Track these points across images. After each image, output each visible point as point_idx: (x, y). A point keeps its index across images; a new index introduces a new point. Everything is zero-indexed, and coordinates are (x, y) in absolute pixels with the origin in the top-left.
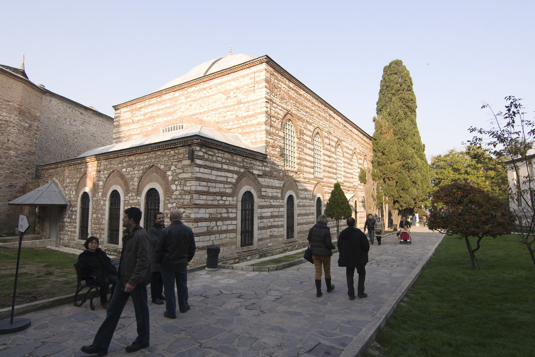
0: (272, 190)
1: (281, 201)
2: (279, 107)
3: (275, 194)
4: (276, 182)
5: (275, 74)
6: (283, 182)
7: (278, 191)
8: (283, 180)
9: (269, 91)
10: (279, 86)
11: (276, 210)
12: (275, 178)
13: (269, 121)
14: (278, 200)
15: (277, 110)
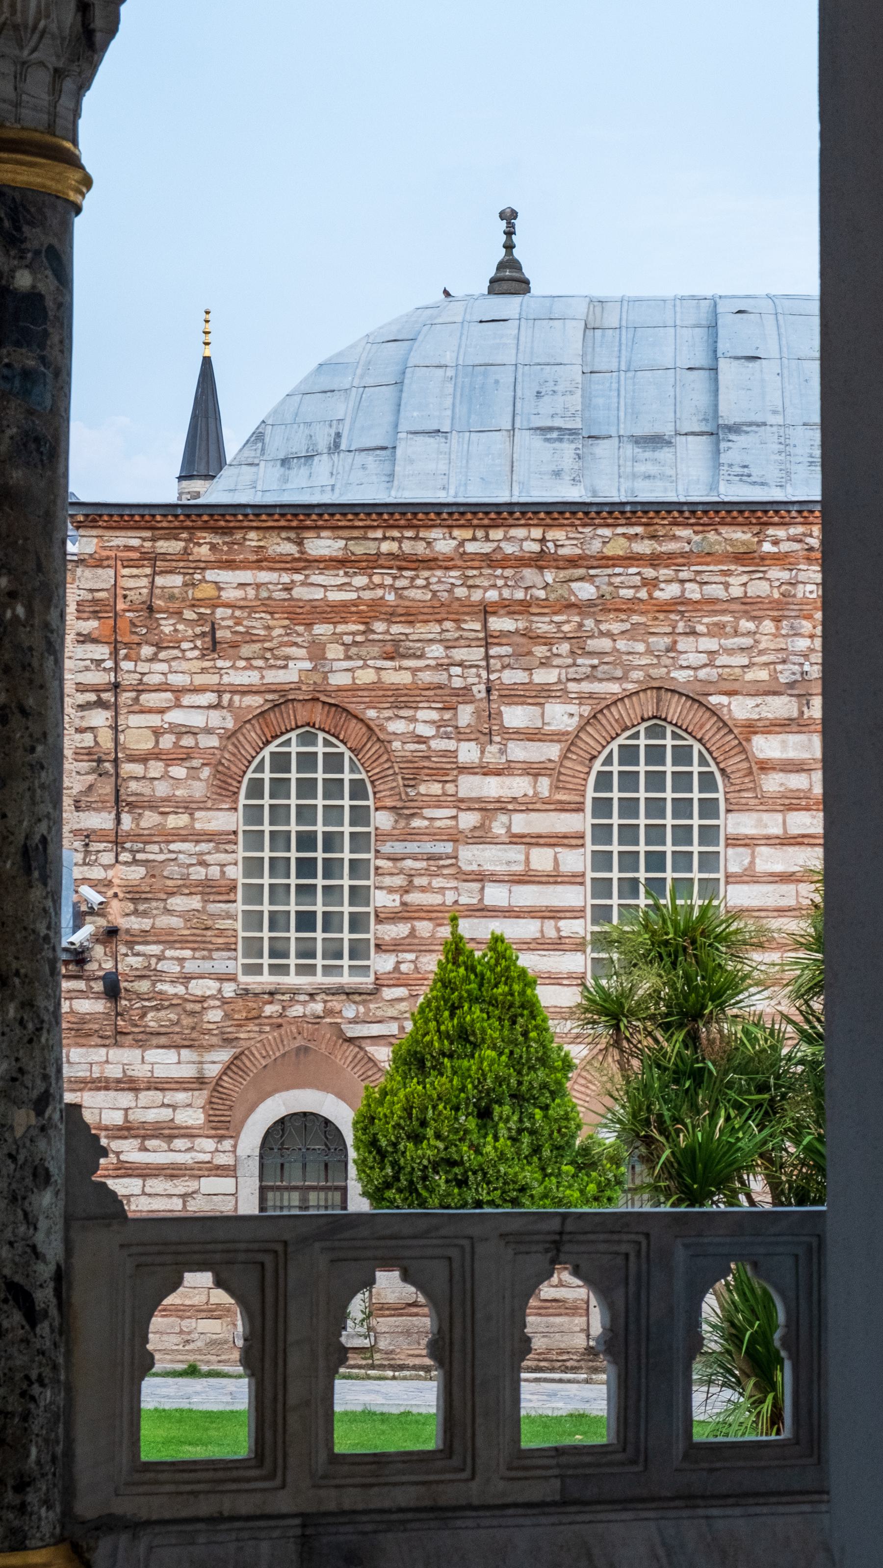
0: (126, 1099)
1: (209, 1144)
2: (187, 700)
3: (152, 1116)
4: (171, 1056)
5: (172, 547)
6: (224, 1055)
7: (181, 1097)
8: (228, 1041)
9: (102, 651)
10: (206, 591)
11: (157, 1185)
12: (144, 1040)
13: (106, 788)
14: (179, 1143)
15: (175, 717)
